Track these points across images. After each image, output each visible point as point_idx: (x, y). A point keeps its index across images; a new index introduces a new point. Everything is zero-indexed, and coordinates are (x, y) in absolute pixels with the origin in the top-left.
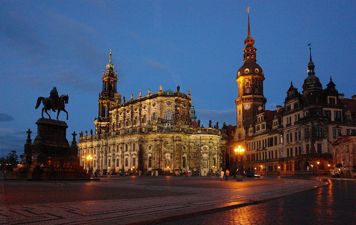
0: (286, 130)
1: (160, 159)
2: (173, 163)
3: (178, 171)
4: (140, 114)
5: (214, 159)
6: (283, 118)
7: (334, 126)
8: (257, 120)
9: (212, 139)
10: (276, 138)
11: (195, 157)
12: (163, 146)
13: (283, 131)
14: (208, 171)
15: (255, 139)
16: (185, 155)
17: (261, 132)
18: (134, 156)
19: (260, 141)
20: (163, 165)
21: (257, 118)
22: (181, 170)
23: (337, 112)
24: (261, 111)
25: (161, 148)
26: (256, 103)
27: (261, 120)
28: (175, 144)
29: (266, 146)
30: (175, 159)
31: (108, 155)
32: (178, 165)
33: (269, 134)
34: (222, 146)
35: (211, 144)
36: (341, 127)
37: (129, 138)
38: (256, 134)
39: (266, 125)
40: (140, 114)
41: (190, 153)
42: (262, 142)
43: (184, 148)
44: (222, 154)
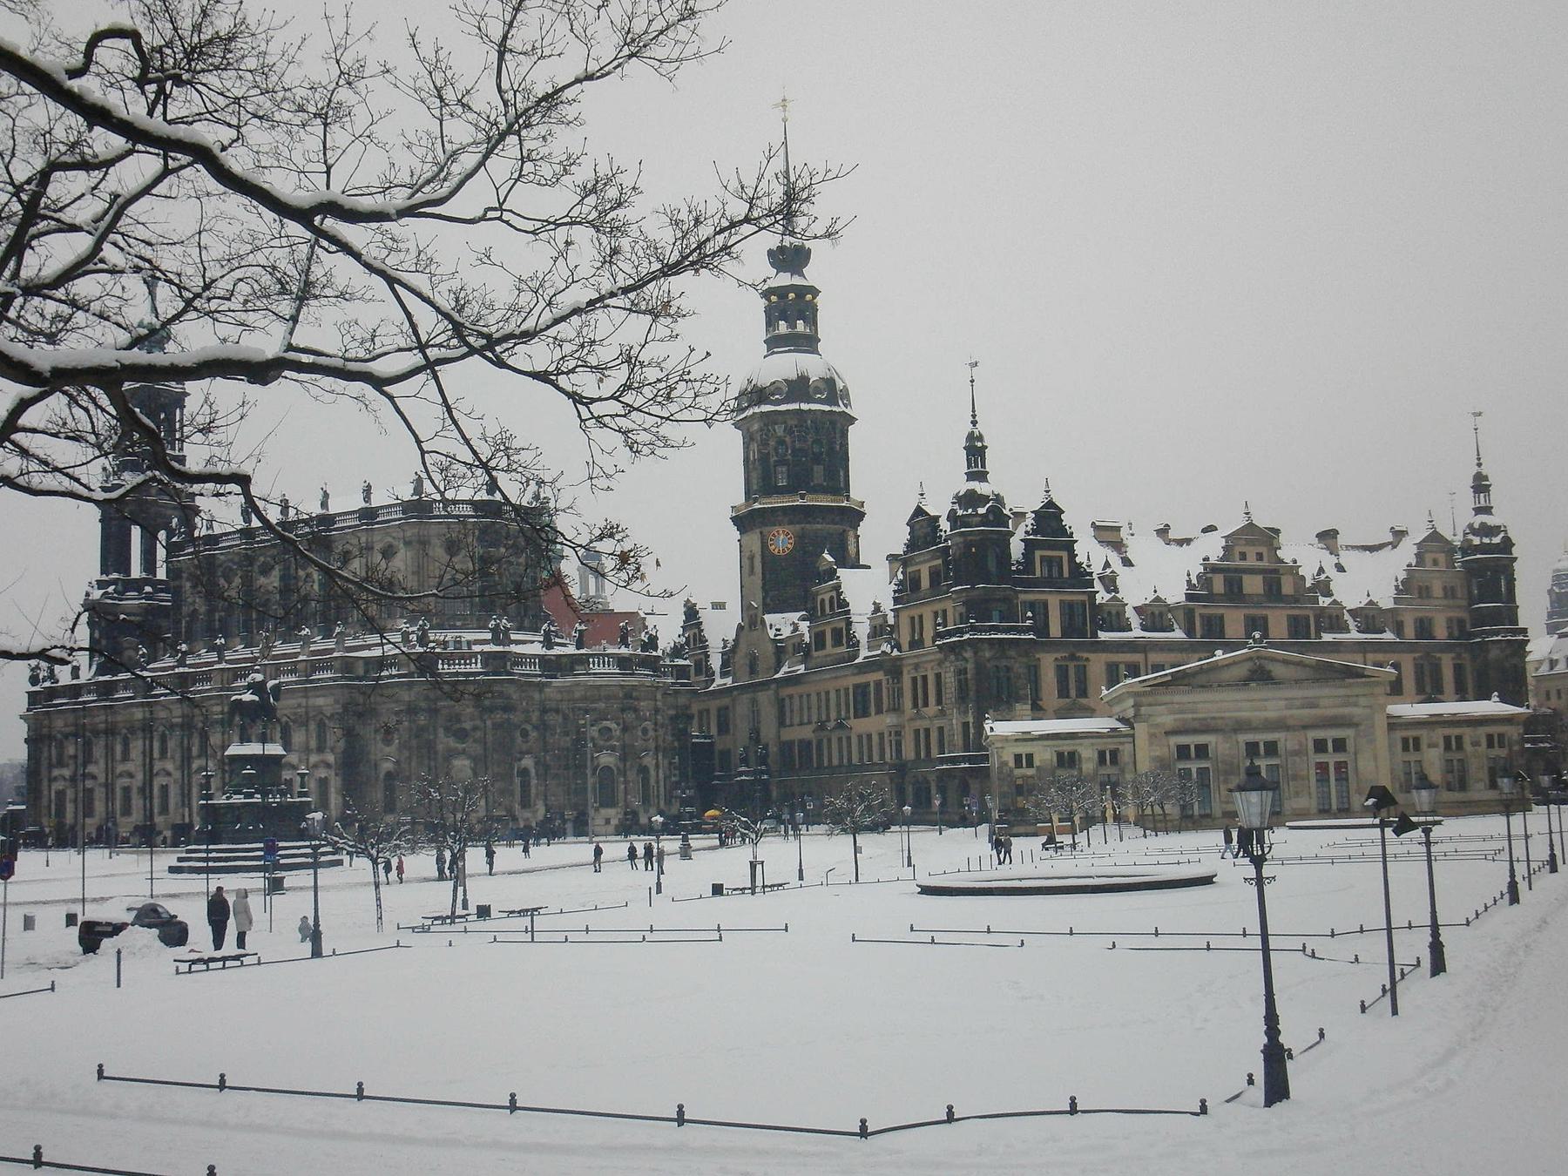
5: (644, 770)
7: (1058, 656)
8: (814, 608)
10: (878, 684)
11: (567, 768)
16: (528, 762)
19: (827, 693)
21: (814, 599)
22: (515, 819)
23: (1071, 605)
28: (489, 723)
29: (848, 711)
31: (195, 766)
34: (672, 712)
36: (1085, 655)
42: (833, 696)
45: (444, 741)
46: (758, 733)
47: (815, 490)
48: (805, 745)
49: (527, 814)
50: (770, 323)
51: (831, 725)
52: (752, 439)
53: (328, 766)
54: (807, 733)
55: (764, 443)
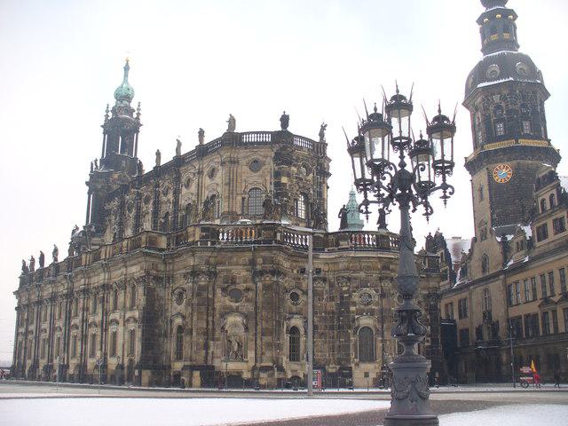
1: (208, 334)
2: (251, 344)
3: (271, 372)
4: (176, 203)
8: (535, 209)
9: (388, 269)
11: (332, 328)
12: (219, 291)
15: (528, 270)
16: (297, 322)
17: (552, 244)
18: (132, 326)
19: (551, 273)
20: (218, 352)
22: (281, 369)
25: (210, 296)
26: (530, 162)
27: (548, 206)
28: (260, 285)
30: (259, 336)
32: (268, 354)
37: (120, 271)
38: (535, 253)
40: (176, 203)
43: (295, 297)
44: (428, 317)
45: (221, 300)
46: (490, 312)
47: (527, 137)
48: (532, 319)
49: (294, 366)
50: (483, 38)
51: (556, 299)
52: (477, 110)
53: (135, 321)
54: (533, 308)
55: (486, 109)
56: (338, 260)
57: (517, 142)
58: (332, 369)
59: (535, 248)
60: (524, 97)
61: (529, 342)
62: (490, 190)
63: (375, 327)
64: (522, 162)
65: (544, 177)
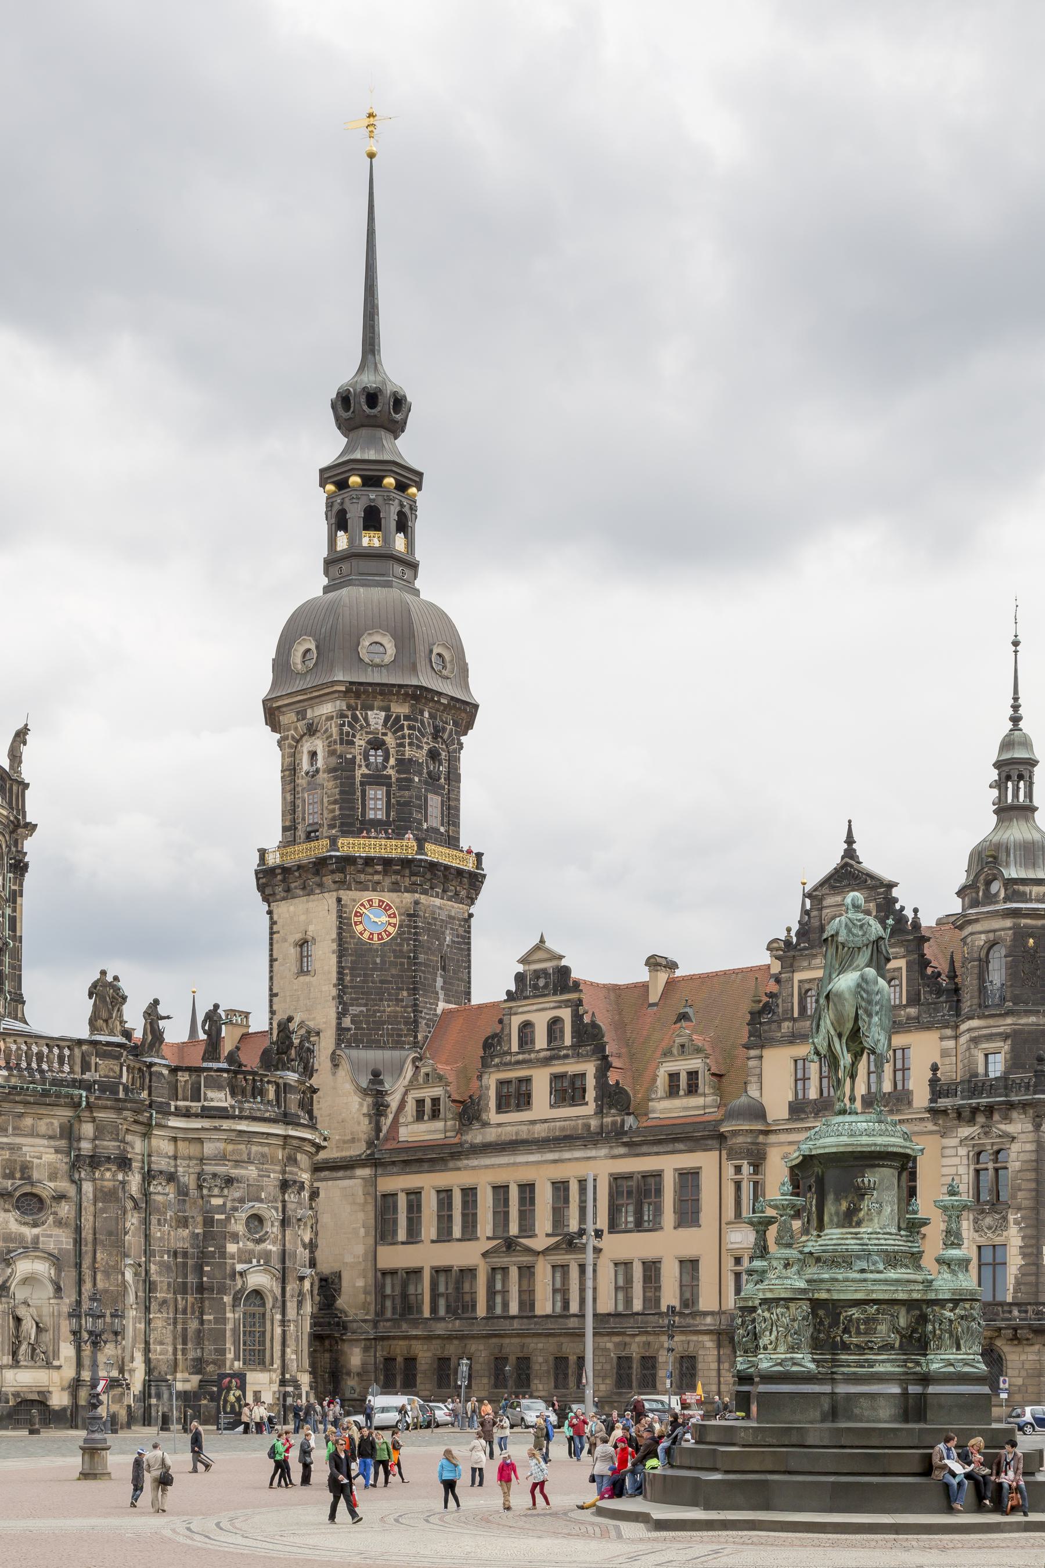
0: (783, 1137)
6: (761, 1057)
11: (183, 1289)
13: (761, 1139)
14: (275, 1387)
15: (458, 1169)
17: (538, 1127)
24: (541, 983)
26: (438, 902)
27: (541, 1040)
33: (622, 1150)
35: (291, 1197)
38: (476, 1136)
39: (591, 1082)
41: (148, 1253)
42: (544, 1197)
51: (539, 1243)
56: (203, 1135)
57: (421, 849)
58: (185, 1382)
59: (485, 1124)
60: (436, 736)
61: (440, 1329)
62: (341, 953)
63: (271, 1291)
64: (423, 899)
65: (537, 975)
